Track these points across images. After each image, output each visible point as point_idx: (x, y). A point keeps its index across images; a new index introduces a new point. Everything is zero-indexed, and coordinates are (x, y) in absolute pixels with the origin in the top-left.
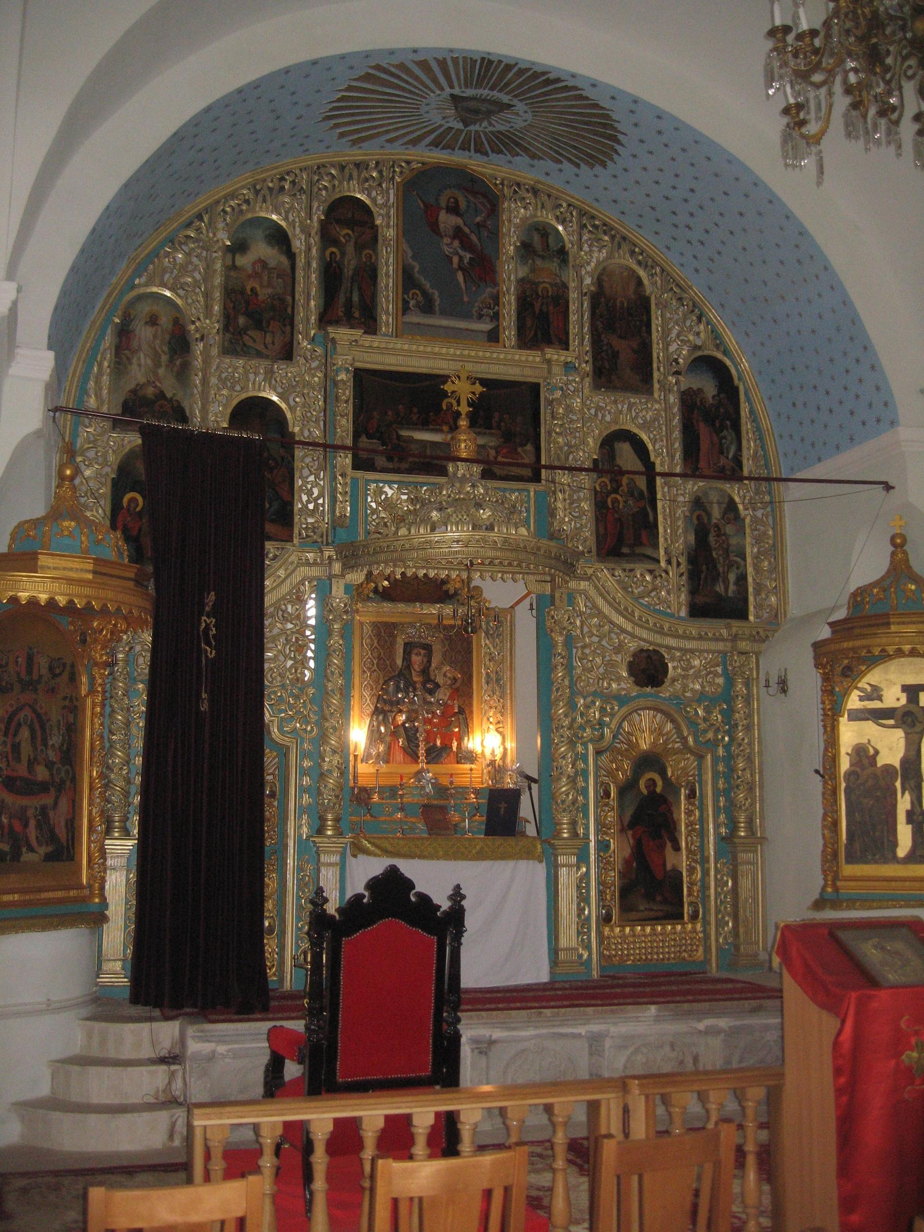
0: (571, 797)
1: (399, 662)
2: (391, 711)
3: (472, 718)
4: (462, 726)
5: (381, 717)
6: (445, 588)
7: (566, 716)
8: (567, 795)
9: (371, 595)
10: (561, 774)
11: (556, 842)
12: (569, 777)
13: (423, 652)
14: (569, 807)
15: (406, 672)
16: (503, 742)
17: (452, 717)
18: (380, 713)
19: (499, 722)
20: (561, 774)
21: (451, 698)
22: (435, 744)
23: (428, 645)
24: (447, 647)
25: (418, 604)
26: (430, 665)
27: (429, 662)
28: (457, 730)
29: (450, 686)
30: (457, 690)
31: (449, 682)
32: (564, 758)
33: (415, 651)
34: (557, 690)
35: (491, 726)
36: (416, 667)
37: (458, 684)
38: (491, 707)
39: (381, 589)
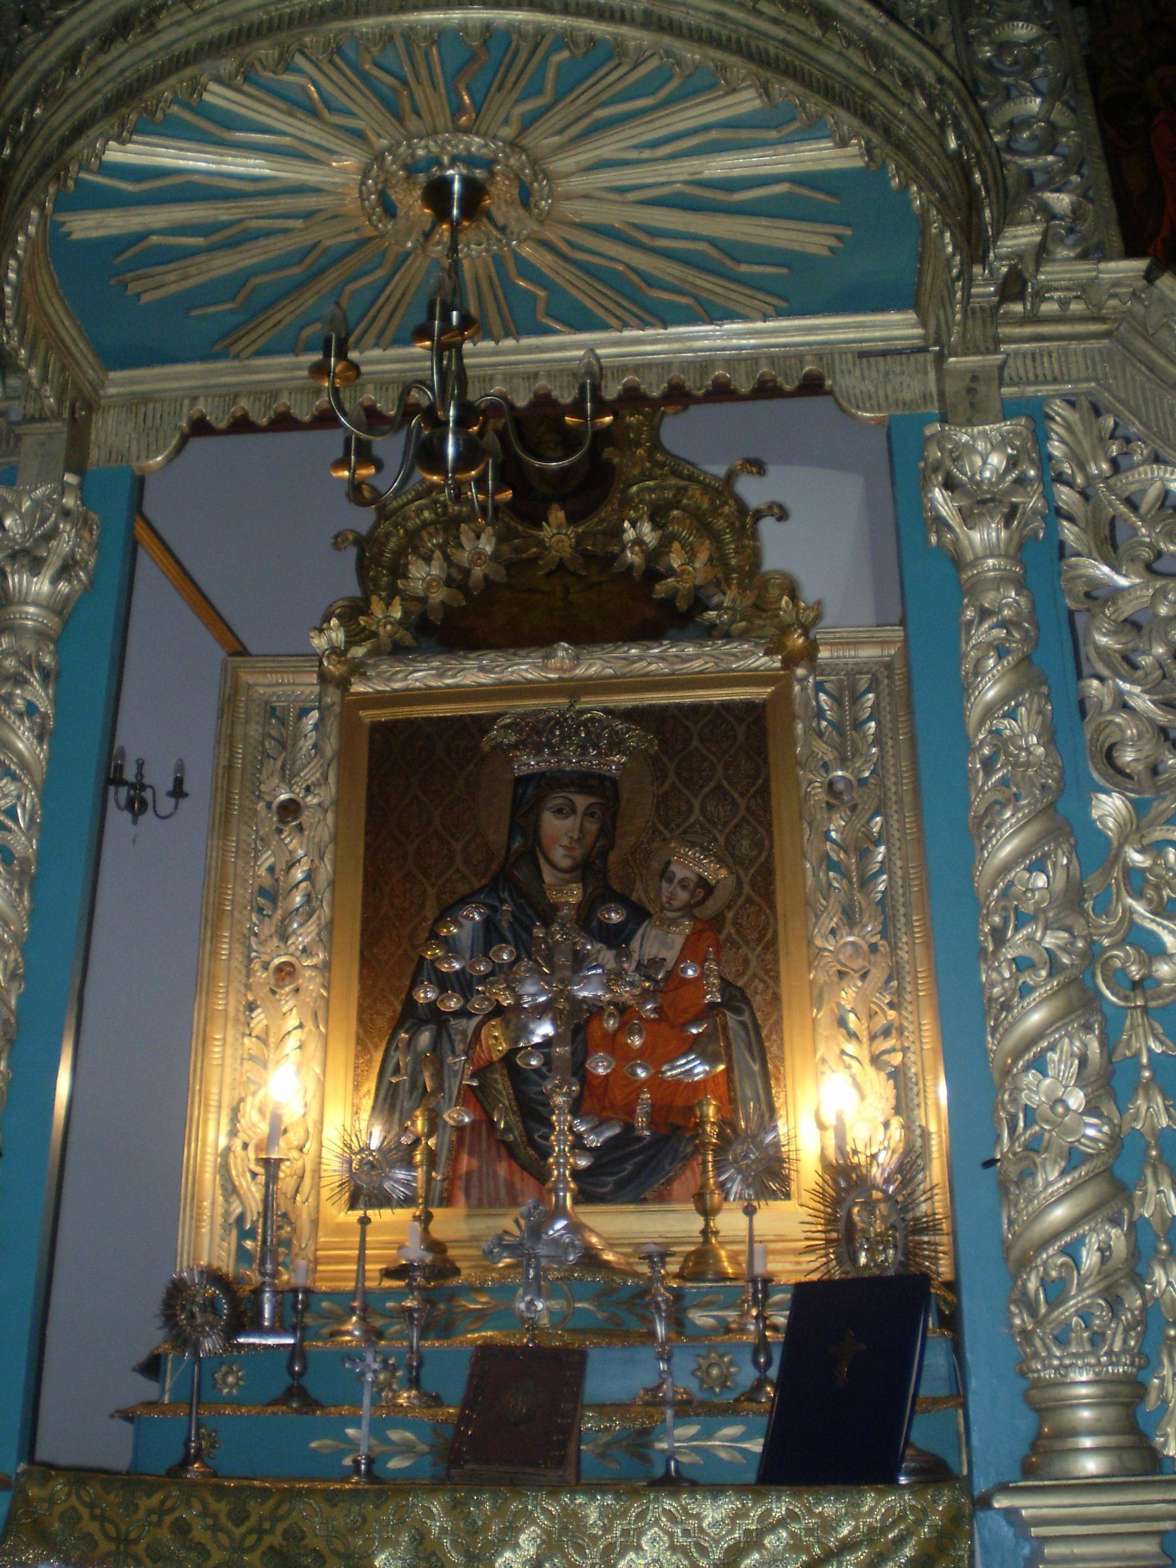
0: (1089, 1259)
1: (497, 836)
2: (463, 1013)
3: (778, 1026)
4: (739, 1050)
5: (425, 1038)
6: (660, 590)
7: (1038, 866)
8: (1072, 1252)
9: (408, 639)
10: (1033, 1147)
11: (1030, 1506)
12: (1073, 1158)
13: (582, 801)
14: (1085, 1315)
15: (522, 874)
16: (903, 1105)
17: (695, 1021)
18: (421, 1023)
19: (886, 1033)
20: (1033, 1147)
21: (690, 951)
22: (629, 1128)
23: (602, 778)
24: (672, 778)
25: (563, 651)
26: (612, 846)
27: (608, 833)
28: (722, 1067)
29: (688, 910)
30: (716, 923)
31: (683, 896)
32: (1039, 1065)
33: (557, 800)
34: (988, 765)
35: (851, 1048)
36: (559, 855)
37: (713, 905)
38: (841, 974)
39: (436, 618)
